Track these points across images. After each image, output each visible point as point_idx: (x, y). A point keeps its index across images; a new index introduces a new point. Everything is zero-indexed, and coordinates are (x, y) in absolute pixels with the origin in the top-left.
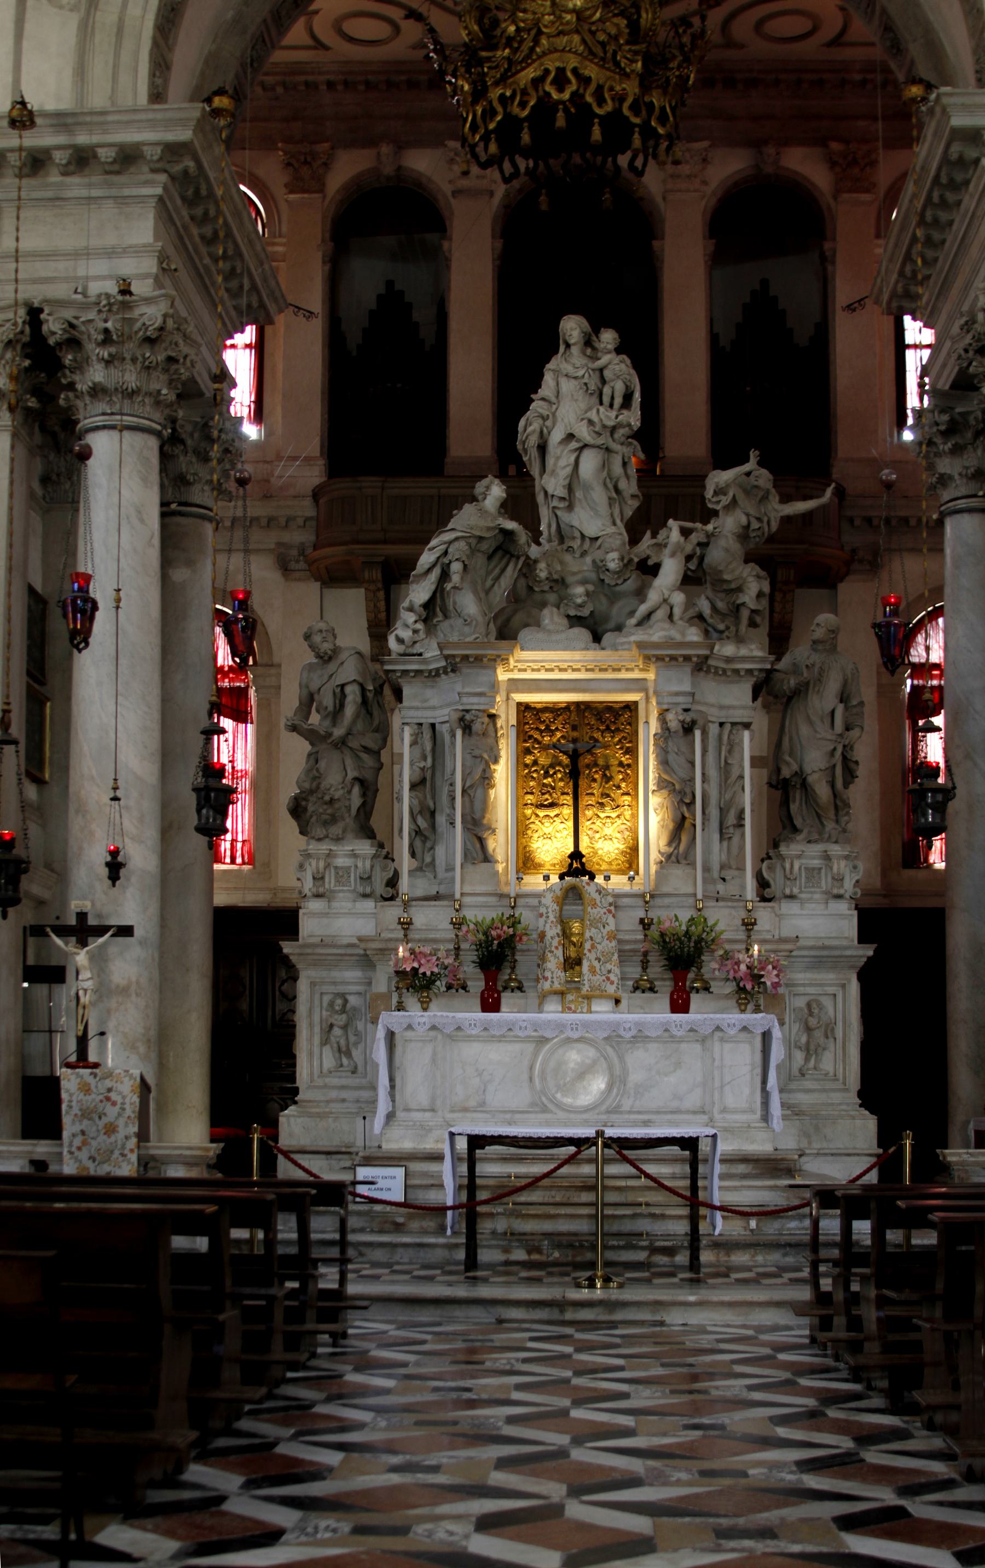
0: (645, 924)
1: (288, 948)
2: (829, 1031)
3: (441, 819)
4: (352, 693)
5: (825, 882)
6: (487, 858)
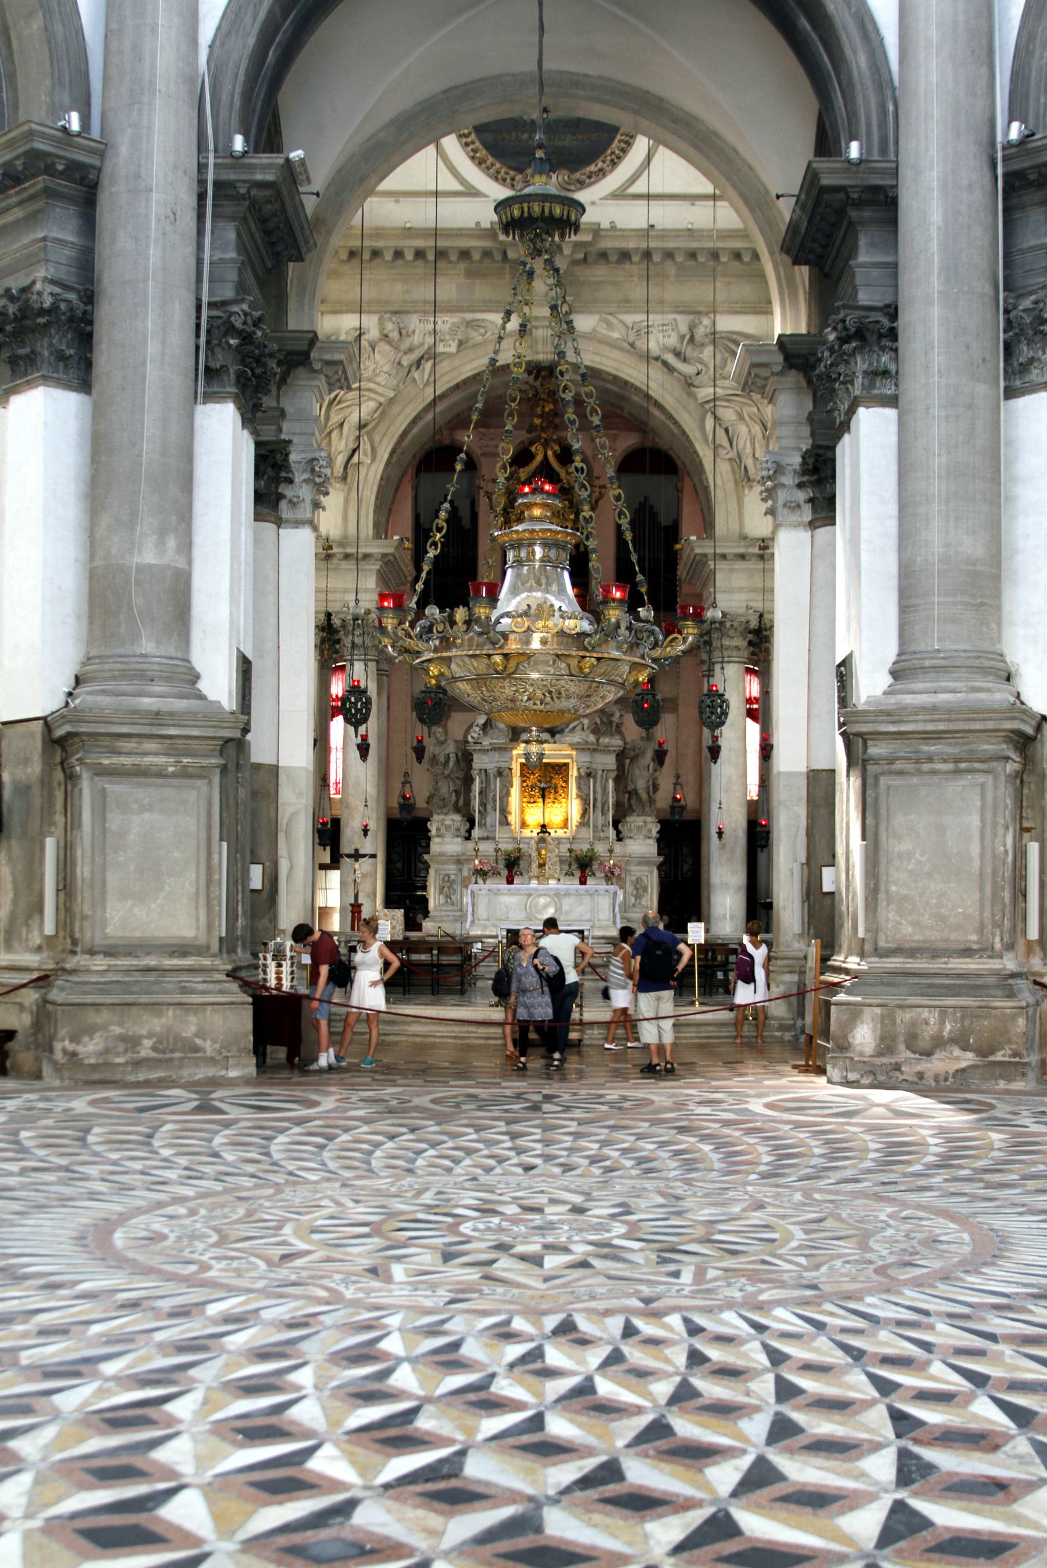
0: (570, 851)
1: (426, 857)
2: (645, 889)
3: (489, 807)
4: (453, 757)
5: (644, 832)
6: (508, 824)
